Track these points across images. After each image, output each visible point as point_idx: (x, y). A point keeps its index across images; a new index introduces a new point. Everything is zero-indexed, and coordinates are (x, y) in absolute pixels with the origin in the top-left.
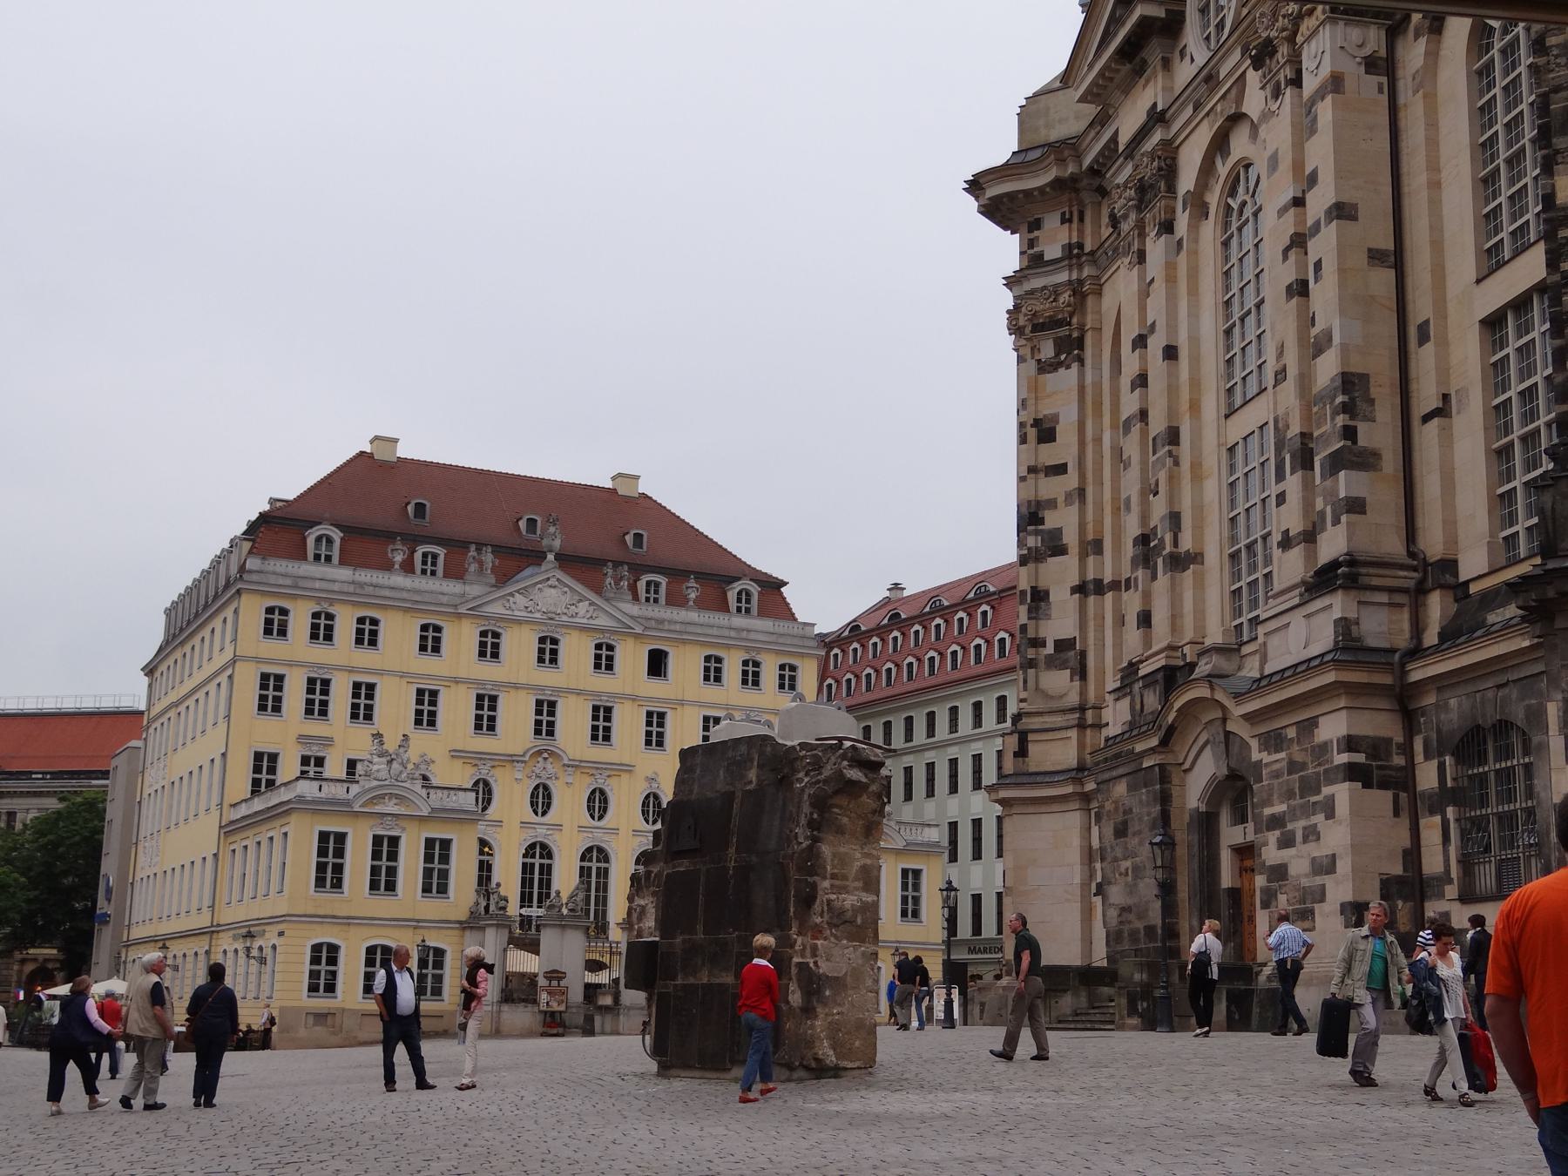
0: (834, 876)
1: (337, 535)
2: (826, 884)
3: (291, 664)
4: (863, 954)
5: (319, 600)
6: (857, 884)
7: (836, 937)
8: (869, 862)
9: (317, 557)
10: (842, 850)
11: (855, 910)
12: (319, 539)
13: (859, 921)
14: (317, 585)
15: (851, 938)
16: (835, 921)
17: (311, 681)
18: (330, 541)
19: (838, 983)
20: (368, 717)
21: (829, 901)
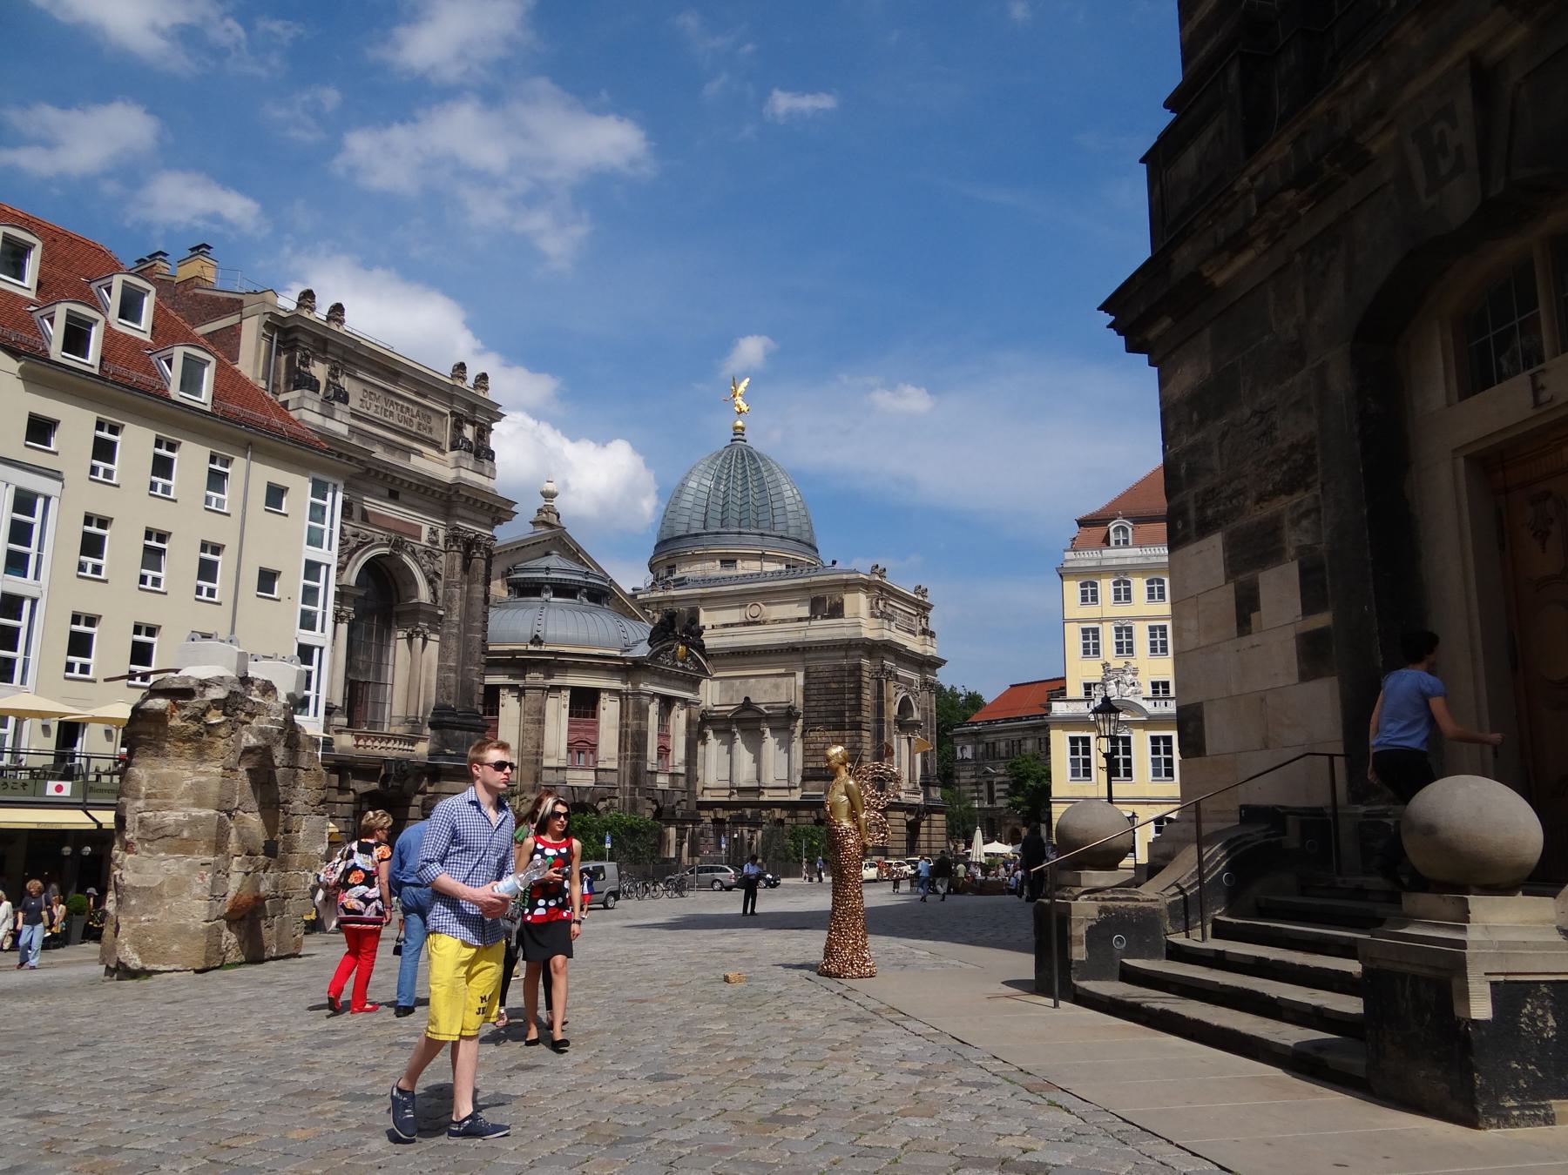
0: (148, 796)
1: (1128, 524)
2: (140, 804)
3: (1101, 621)
4: (189, 865)
5: (1116, 573)
6: (185, 800)
7: (149, 850)
8: (203, 779)
9: (1117, 542)
10: (165, 770)
11: (180, 826)
12: (1116, 530)
13: (186, 834)
14: (1114, 562)
15: (170, 850)
16: (150, 836)
17: (1118, 630)
18: (1125, 531)
19: (151, 894)
20: (1097, 652)
21: (141, 821)
